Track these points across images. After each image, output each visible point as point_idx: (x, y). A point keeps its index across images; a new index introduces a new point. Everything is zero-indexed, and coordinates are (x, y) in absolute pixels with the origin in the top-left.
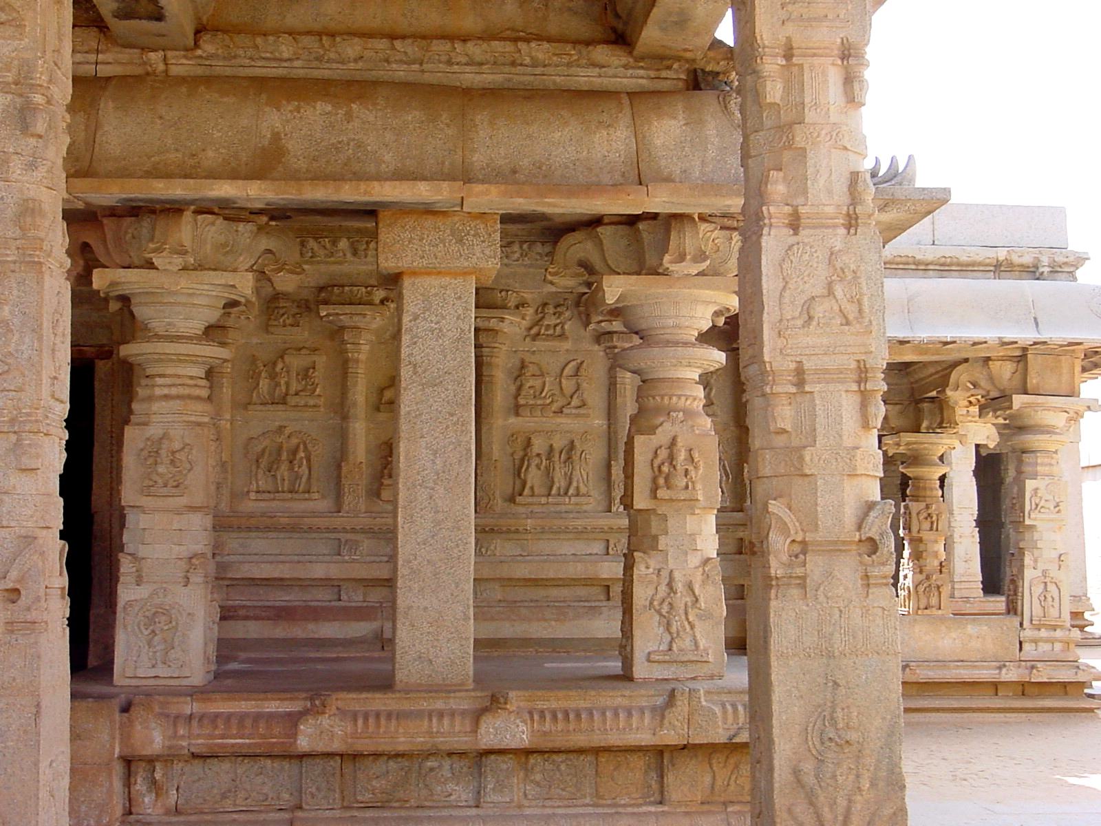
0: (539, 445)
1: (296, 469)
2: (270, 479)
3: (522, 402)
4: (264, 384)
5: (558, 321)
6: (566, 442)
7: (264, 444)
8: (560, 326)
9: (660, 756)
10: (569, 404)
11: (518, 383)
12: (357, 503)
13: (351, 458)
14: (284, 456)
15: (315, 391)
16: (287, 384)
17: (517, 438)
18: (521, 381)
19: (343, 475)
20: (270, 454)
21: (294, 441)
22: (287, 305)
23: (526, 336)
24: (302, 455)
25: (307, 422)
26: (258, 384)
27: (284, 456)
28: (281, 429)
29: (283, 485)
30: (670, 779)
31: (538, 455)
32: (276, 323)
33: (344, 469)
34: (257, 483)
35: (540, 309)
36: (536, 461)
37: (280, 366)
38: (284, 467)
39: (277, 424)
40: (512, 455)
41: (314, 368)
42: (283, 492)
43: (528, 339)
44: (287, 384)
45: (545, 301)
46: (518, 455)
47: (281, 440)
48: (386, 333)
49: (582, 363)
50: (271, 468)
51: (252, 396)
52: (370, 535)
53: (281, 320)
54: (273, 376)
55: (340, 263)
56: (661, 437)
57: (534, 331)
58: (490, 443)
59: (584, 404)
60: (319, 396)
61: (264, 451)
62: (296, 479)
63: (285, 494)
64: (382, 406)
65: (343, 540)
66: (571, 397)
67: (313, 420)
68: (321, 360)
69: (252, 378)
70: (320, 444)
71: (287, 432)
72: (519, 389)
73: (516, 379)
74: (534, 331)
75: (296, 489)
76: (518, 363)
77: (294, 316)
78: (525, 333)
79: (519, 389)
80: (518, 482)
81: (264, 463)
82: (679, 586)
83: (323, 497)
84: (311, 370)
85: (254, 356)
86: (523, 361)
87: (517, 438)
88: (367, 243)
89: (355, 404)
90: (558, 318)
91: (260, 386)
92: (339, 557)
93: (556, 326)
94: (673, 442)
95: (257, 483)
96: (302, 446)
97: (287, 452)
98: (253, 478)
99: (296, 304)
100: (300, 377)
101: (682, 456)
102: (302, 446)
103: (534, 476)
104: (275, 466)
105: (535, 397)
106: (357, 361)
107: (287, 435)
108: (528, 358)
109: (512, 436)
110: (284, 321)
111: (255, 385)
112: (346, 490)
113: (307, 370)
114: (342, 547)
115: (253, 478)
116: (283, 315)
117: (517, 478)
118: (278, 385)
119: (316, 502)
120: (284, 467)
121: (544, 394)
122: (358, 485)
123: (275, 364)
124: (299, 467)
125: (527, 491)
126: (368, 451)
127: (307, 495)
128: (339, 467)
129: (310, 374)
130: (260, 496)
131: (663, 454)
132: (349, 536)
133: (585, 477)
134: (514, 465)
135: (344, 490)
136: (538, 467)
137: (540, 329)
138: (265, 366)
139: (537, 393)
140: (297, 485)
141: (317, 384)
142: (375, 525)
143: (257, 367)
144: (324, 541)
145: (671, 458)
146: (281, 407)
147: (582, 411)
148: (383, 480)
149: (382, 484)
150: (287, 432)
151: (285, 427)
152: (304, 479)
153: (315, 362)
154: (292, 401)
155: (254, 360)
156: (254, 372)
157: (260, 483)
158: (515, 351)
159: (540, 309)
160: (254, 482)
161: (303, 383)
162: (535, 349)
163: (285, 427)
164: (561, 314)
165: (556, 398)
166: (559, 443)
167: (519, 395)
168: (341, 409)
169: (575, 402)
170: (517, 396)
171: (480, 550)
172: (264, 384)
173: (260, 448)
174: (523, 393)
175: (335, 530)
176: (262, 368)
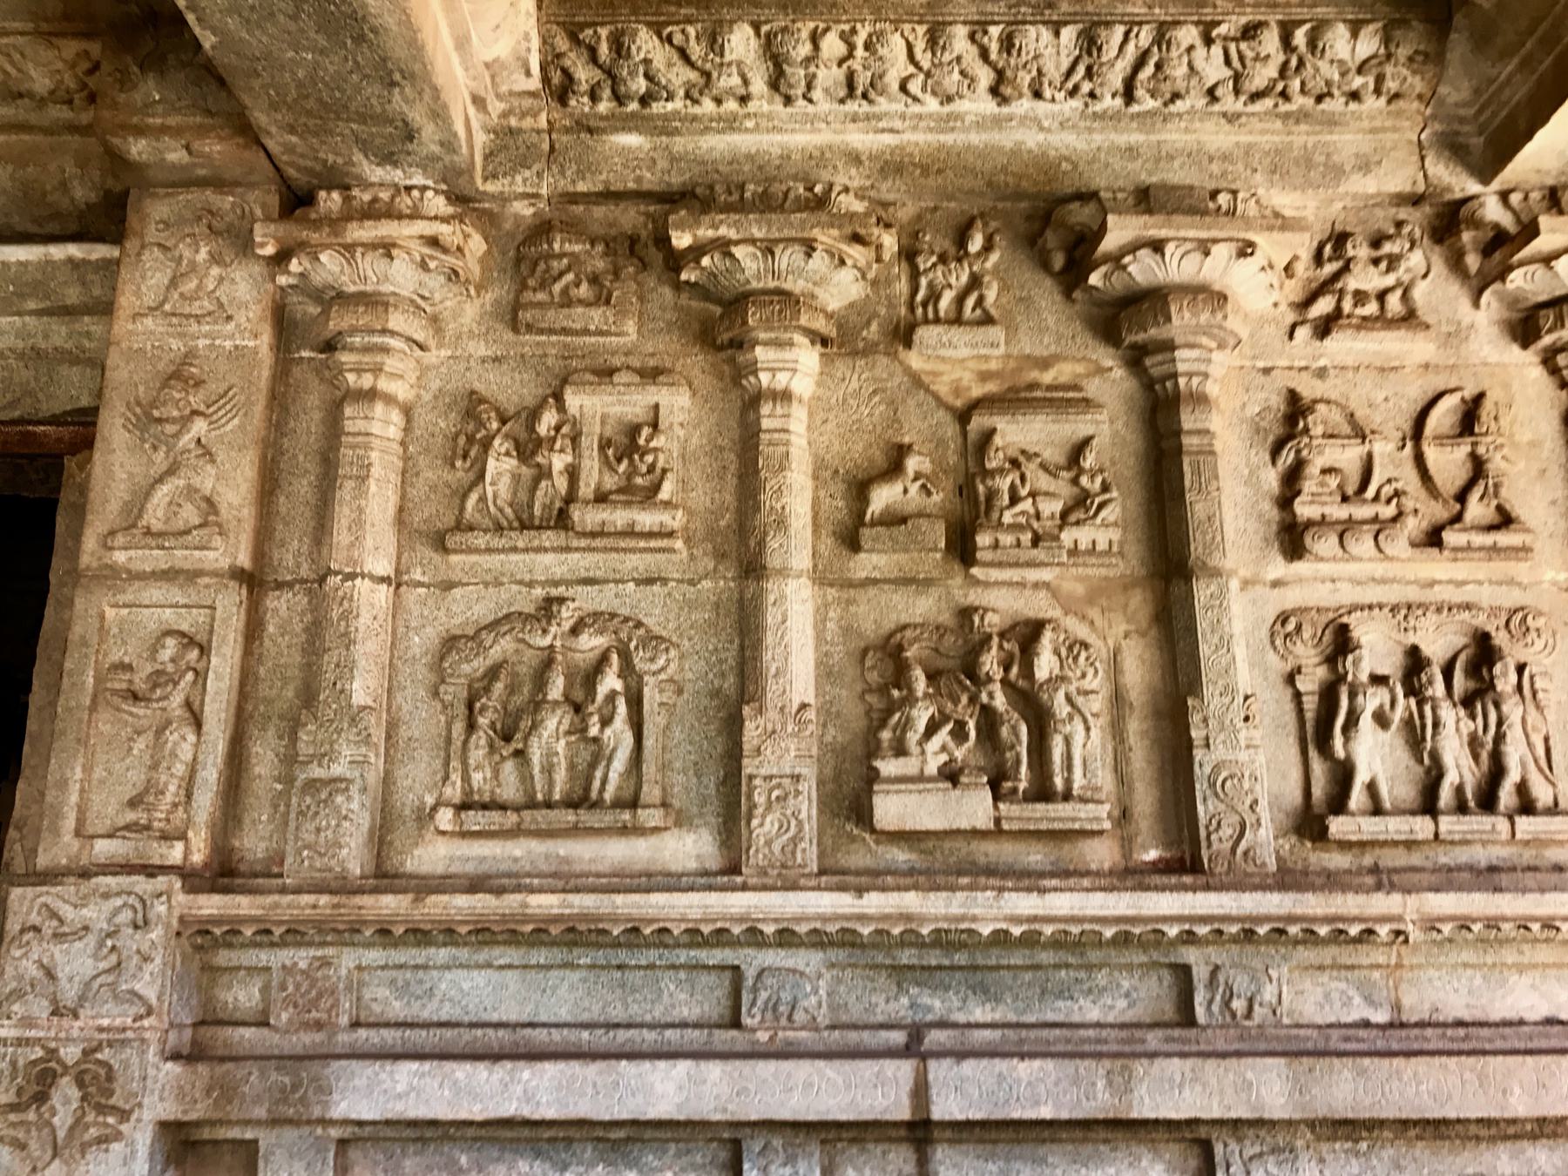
0: (1377, 649)
1: (594, 731)
2: (509, 767)
3: (1304, 509)
4: (501, 466)
5: (1390, 280)
6: (1461, 641)
7: (495, 653)
8: (1399, 292)
10: (1457, 518)
11: (1287, 457)
12: (795, 841)
13: (772, 689)
14: (556, 689)
15: (657, 487)
16: (573, 473)
17: (1299, 628)
18: (1298, 452)
19: (746, 747)
20: (512, 689)
21: (591, 643)
22: (577, 248)
23: (1293, 328)
24: (618, 685)
25: (631, 585)
26: (481, 476)
27: (556, 689)
28: (548, 608)
29: (551, 783)
31: (1378, 680)
32: (541, 296)
33: (751, 732)
34: (466, 778)
35: (1328, 249)
36: (1373, 699)
37: (548, 419)
38: (554, 723)
39: (539, 592)
40: (1290, 679)
41: (655, 426)
42: (549, 805)
43: (1303, 333)
44: (573, 473)
45: (1338, 228)
46: (1309, 683)
47: (547, 641)
48: (868, 323)
49: (1479, 398)
50: (516, 729)
51: (462, 509)
52: (839, 955)
53: (557, 288)
54: (529, 447)
55: (731, 124)
57: (1324, 306)
58: (1226, 643)
59: (1505, 520)
60: (667, 504)
61: (493, 673)
62: (593, 766)
63: (553, 814)
64: (866, 534)
65: (750, 974)
66: (1462, 497)
67: (650, 581)
68: (676, 402)
69: (465, 457)
70: (673, 653)
71: (568, 615)
72: (1292, 479)
73: (1275, 452)
74: (1324, 306)
75: (594, 795)
76: (1278, 402)
77: (594, 280)
78: (1291, 317)
79: (1292, 479)
80: (1318, 767)
83: (682, 821)
84: (646, 431)
85: (473, 392)
86: (1293, 397)
87: (1299, 628)
88: (815, 39)
89: (781, 523)
90: (1389, 270)
91: (488, 478)
92: (734, 1033)
93: (1382, 296)
95: (466, 778)
96: (615, 657)
97: (569, 677)
98: (455, 763)
99: (600, 248)
100: (610, 452)
102: (615, 657)
103: (1375, 755)
104: (525, 724)
105: (1345, 499)
106: (785, 396)
107: (567, 625)
108: (1308, 388)
109: (1283, 623)
110: (565, 291)
111: (472, 476)
112: (760, 798)
113: (634, 430)
114: (746, 998)
115: (455, 763)
116: (561, 274)
117: (1313, 753)
118: (544, 473)
119: (653, 840)
120: (554, 723)
121: (1370, 493)
122: (796, 778)
123: (534, 415)
124: (606, 722)
125: (1357, 798)
126: (826, 673)
127: (626, 816)
128: (733, 726)
129: (641, 442)
130: (476, 821)
132: (771, 957)
133: (1541, 752)
134: (1300, 711)
135: (750, 796)
136: (1381, 719)
137: (1339, 301)
138: (504, 422)
139: (1350, 491)
140: (596, 784)
141: (664, 471)
142: (862, 918)
143: (481, 424)
144: (682, 975)
146: (549, 538)
147: (1503, 538)
148: (878, 764)
149: (873, 776)
150: (568, 615)
151: (561, 600)
152: (619, 764)
153: (656, 407)
154: (586, 516)
156: (471, 439)
157: (477, 778)
158: (1267, 371)
159: (1328, 249)
160: (456, 777)
161: (622, 468)
162: (1322, 363)
163: (561, 600)
164: (1393, 262)
165: (1409, 504)
166: (1439, 641)
167: (1299, 493)
168: (744, 553)
169: (1476, 509)
170: (1286, 501)
171: (1227, 1003)
172: (501, 466)
173: (479, 665)
174: (1309, 486)
175: (721, 937)
176: (495, 425)
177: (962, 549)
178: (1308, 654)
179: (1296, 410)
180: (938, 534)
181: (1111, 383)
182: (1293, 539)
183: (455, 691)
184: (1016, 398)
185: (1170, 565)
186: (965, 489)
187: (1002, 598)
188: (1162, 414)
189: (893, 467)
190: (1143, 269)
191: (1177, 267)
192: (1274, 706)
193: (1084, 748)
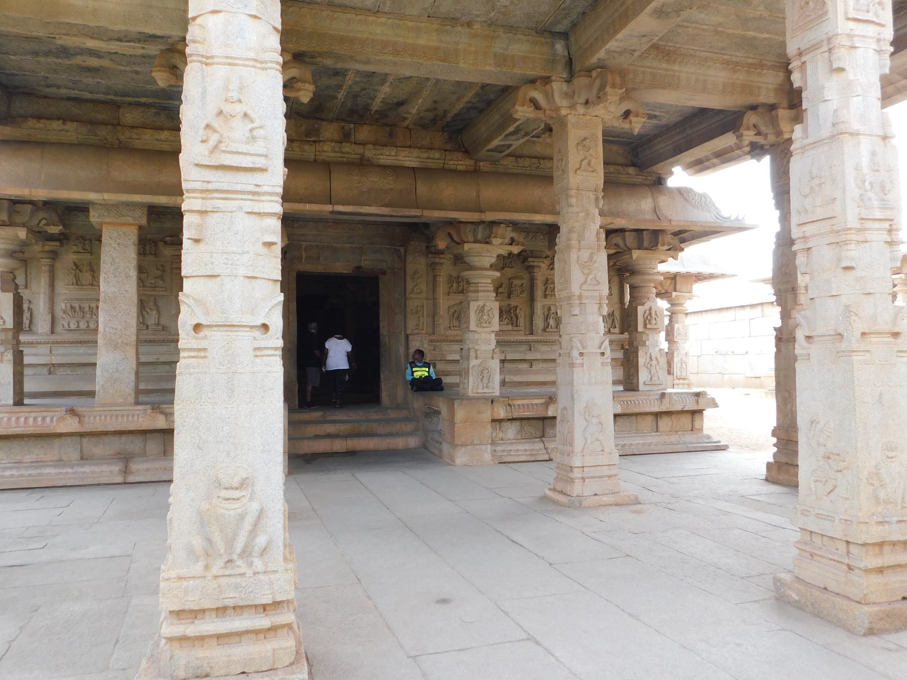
4: (455, 285)
9: (657, 415)
30: (660, 423)
56: (647, 306)
81: (456, 315)
82: (653, 358)
94: (650, 309)
101: (653, 313)
131: (647, 312)
145: (650, 314)
155: (450, 276)
172: (455, 285)
177: (509, 297)
178: (546, 310)
179: (547, 280)
180: (506, 295)
181: (526, 276)
182: (545, 296)
183: (451, 313)
184: (516, 278)
185: (532, 300)
186: (509, 289)
187: (513, 304)
188: (532, 280)
189: (501, 286)
190: (532, 264)
191: (535, 264)
192: (542, 316)
193: (521, 321)
